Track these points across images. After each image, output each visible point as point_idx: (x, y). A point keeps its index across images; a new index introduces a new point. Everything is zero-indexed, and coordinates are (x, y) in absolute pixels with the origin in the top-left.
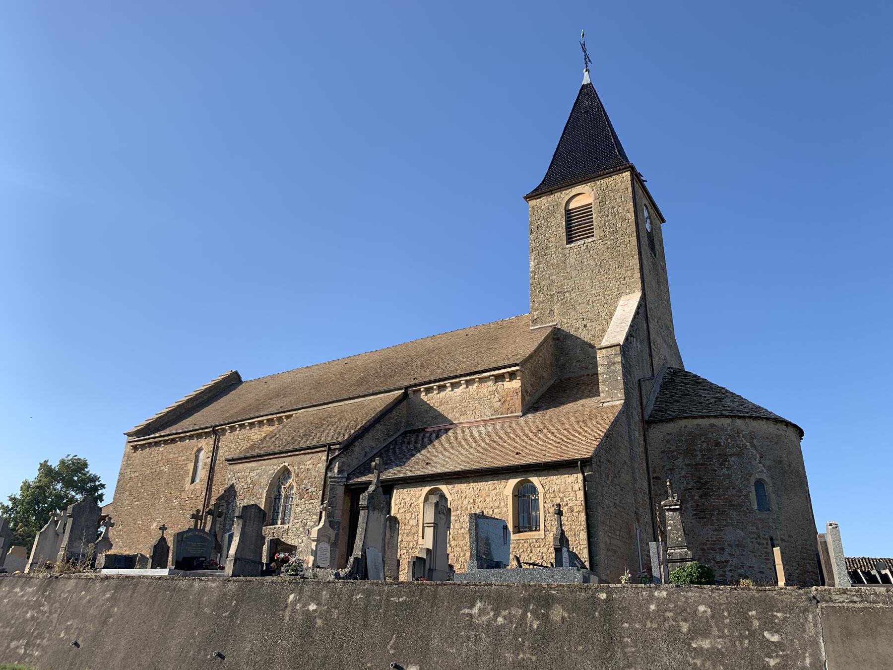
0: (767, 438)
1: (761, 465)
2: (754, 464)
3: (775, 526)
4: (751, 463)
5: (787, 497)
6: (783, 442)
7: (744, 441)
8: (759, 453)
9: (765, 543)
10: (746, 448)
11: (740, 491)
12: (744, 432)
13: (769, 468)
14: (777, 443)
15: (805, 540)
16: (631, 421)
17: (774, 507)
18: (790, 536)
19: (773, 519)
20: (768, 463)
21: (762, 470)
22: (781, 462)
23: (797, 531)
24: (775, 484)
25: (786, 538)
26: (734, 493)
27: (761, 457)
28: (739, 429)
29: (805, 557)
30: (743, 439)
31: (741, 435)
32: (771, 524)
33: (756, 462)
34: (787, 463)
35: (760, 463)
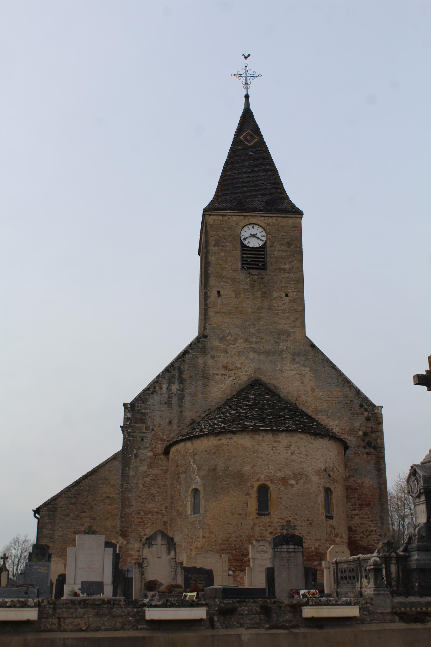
0: (206, 451)
1: (198, 477)
2: (193, 477)
3: (199, 526)
4: (190, 476)
5: (215, 499)
6: (223, 450)
7: (190, 459)
8: (198, 466)
9: (191, 542)
10: (190, 464)
11: (183, 502)
12: (190, 451)
13: (202, 478)
14: (214, 453)
15: (229, 533)
16: (133, 460)
17: (202, 510)
18: (210, 533)
19: (200, 521)
20: (203, 473)
21: (198, 480)
22: (214, 470)
23: (220, 527)
24: (205, 490)
25: (207, 535)
26: (181, 503)
27: (198, 470)
28: (188, 449)
29: (225, 548)
30: (189, 457)
31: (188, 454)
32: (197, 525)
33: (194, 475)
34: (221, 469)
35: (197, 475)
